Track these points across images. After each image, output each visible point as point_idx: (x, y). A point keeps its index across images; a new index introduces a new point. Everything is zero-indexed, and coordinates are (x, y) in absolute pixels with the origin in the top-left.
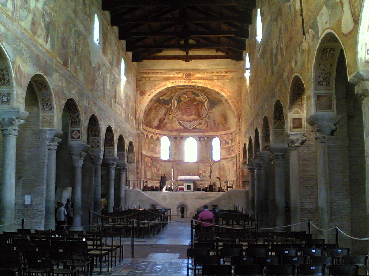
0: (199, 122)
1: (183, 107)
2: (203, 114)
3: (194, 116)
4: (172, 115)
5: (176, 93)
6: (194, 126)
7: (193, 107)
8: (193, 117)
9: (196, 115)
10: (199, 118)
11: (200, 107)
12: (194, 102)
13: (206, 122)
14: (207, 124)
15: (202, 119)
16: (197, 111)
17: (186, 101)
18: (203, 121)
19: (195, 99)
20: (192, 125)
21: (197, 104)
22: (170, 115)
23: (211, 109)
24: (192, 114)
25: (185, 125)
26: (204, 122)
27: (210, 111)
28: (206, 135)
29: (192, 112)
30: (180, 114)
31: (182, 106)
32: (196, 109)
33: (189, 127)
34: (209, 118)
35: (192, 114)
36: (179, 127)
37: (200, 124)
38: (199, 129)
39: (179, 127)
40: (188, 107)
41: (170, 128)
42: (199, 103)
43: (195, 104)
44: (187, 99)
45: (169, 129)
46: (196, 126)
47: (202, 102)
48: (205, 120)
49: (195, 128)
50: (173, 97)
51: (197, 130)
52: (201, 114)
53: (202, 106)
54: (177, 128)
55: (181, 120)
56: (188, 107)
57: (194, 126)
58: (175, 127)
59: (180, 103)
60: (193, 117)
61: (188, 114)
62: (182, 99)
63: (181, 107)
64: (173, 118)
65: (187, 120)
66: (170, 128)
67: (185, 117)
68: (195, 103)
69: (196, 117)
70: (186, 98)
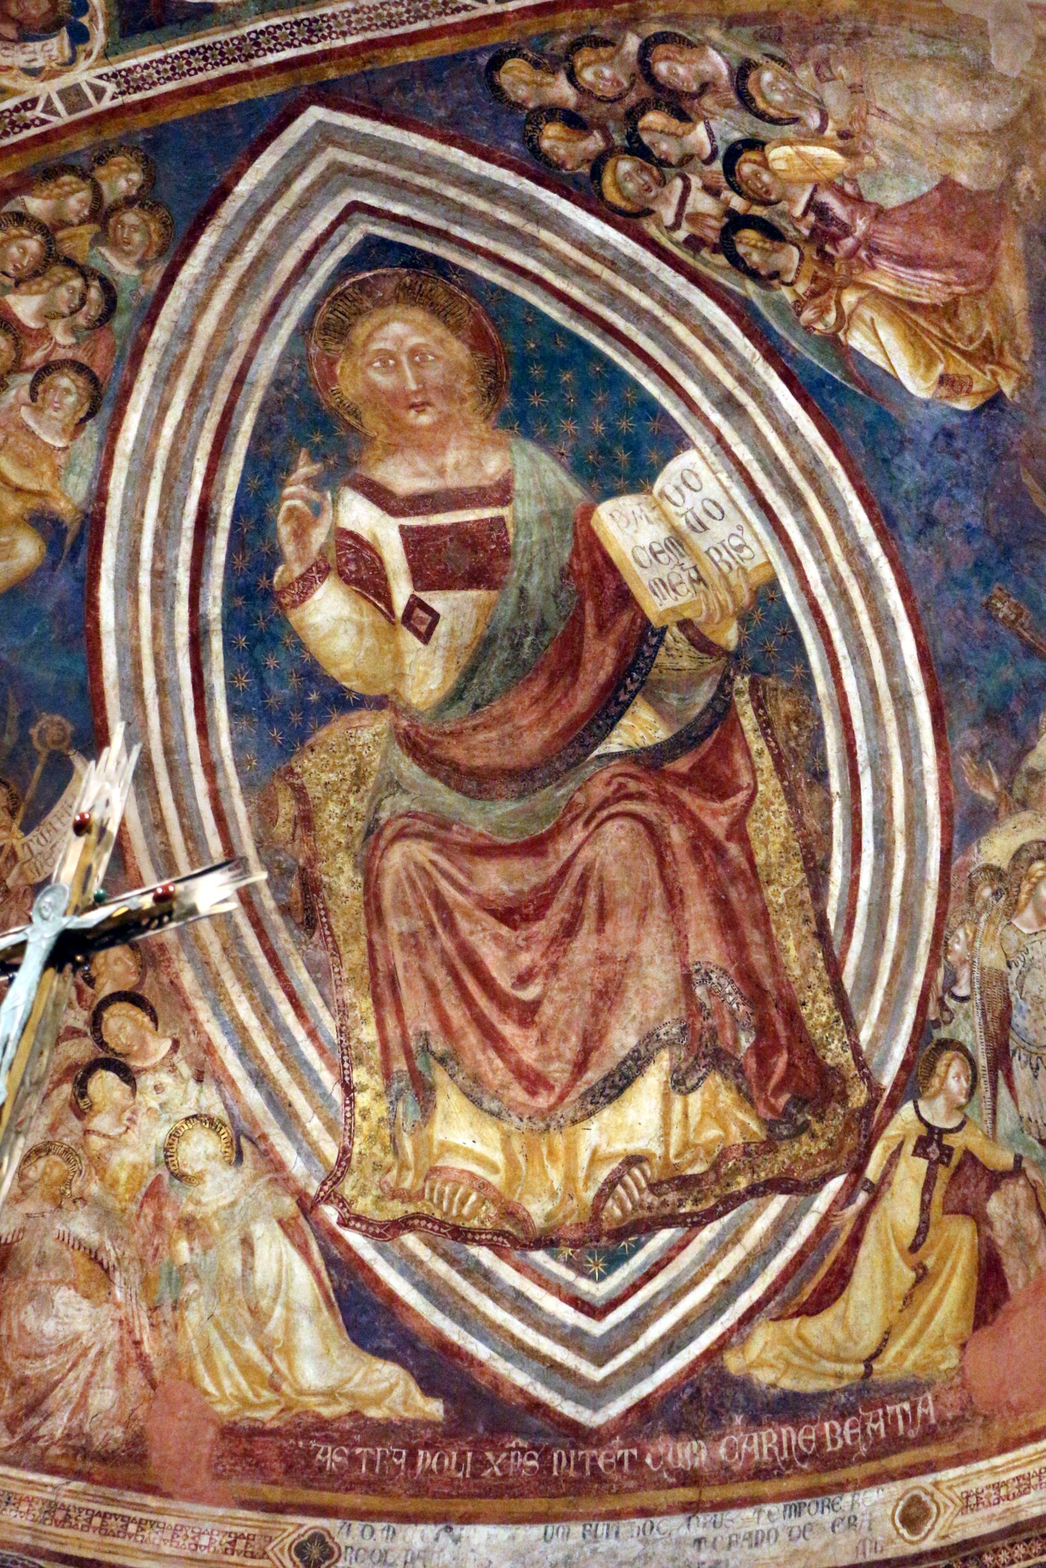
0: (782, 1229)
1: (396, 858)
2: (868, 980)
3: (679, 1083)
4: (172, 1091)
5: (104, 401)
6: (670, 1345)
7: (612, 848)
8: (638, 1121)
9: (703, 1056)
10: (779, 1129)
11: (772, 831)
12: (609, 709)
13: (961, 1180)
14: (981, 1220)
15: (867, 1127)
16: (708, 948)
17: (426, 675)
18: (876, 1192)
19: (596, 575)
20: (639, 1321)
21: (703, 753)
22: (105, 1085)
23: (1011, 768)
24: (623, 1039)
25: (489, 1331)
26: (902, 1207)
27: (997, 848)
28: (977, 1524)
29: (608, 995)
30: (344, 1056)
31: (373, 837)
32: (698, 907)
33: (552, 1371)
34: (1001, 1058)
35: (623, 1039)
36: (324, 1369)
37: (818, 1282)
38: (790, 1407)
39: (324, 1369)
40: (495, 878)
41: (104, 1403)
42: (721, 713)
43: (649, 760)
44: (421, 621)
45: (58, 1425)
46: (722, 1344)
47: (768, 640)
48: (930, 1140)
49: (706, 1399)
50: (93, 523)
51: (763, 1443)
52: (818, 1011)
53: (802, 768)
54: (267, 1416)
55: (363, 1205)
56: (495, 878)
57: (670, 1345)
58: (226, 1389)
59: (315, 769)
60: (638, 1121)
61: (529, 1056)
62: (328, 616)
63: (343, 879)
64: (201, 1149)
65: (510, 1212)
66: (104, 1399)
67: (465, 1136)
68: (641, 727)
69: (716, 1117)
70: (402, 592)
